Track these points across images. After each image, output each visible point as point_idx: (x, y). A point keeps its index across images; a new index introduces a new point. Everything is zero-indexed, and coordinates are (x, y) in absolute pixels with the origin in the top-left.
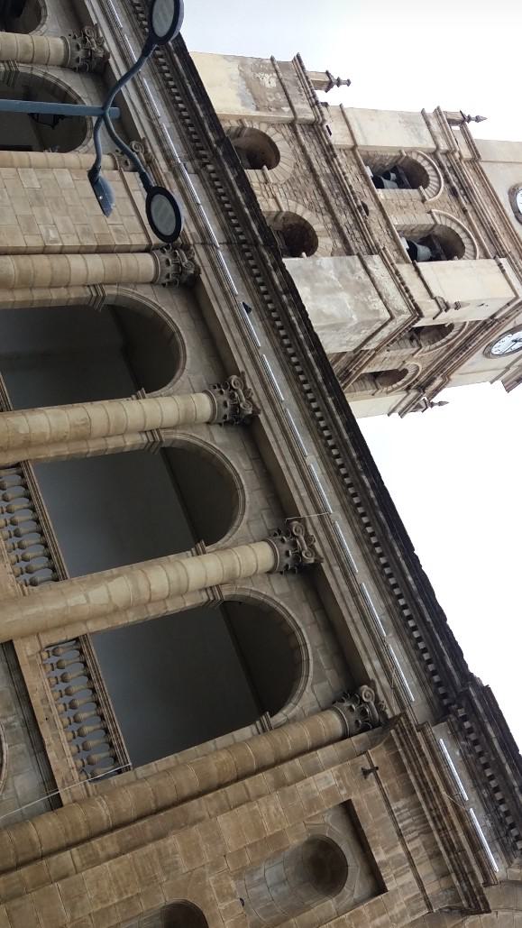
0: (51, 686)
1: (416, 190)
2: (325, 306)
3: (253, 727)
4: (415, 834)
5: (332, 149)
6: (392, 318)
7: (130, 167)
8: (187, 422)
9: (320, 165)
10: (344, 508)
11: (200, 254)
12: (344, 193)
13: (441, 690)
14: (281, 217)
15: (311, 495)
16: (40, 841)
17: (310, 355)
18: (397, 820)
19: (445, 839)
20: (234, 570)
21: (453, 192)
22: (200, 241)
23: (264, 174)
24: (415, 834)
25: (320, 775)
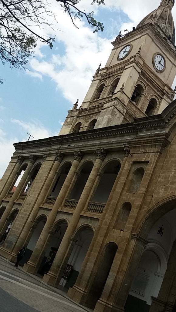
1: (104, 88)
6: (114, 106)
8: (76, 167)
10: (101, 139)
12: (92, 109)
13: (135, 131)
14: (89, 127)
17: (78, 136)
20: (95, 168)
21: (109, 77)
23: (81, 127)
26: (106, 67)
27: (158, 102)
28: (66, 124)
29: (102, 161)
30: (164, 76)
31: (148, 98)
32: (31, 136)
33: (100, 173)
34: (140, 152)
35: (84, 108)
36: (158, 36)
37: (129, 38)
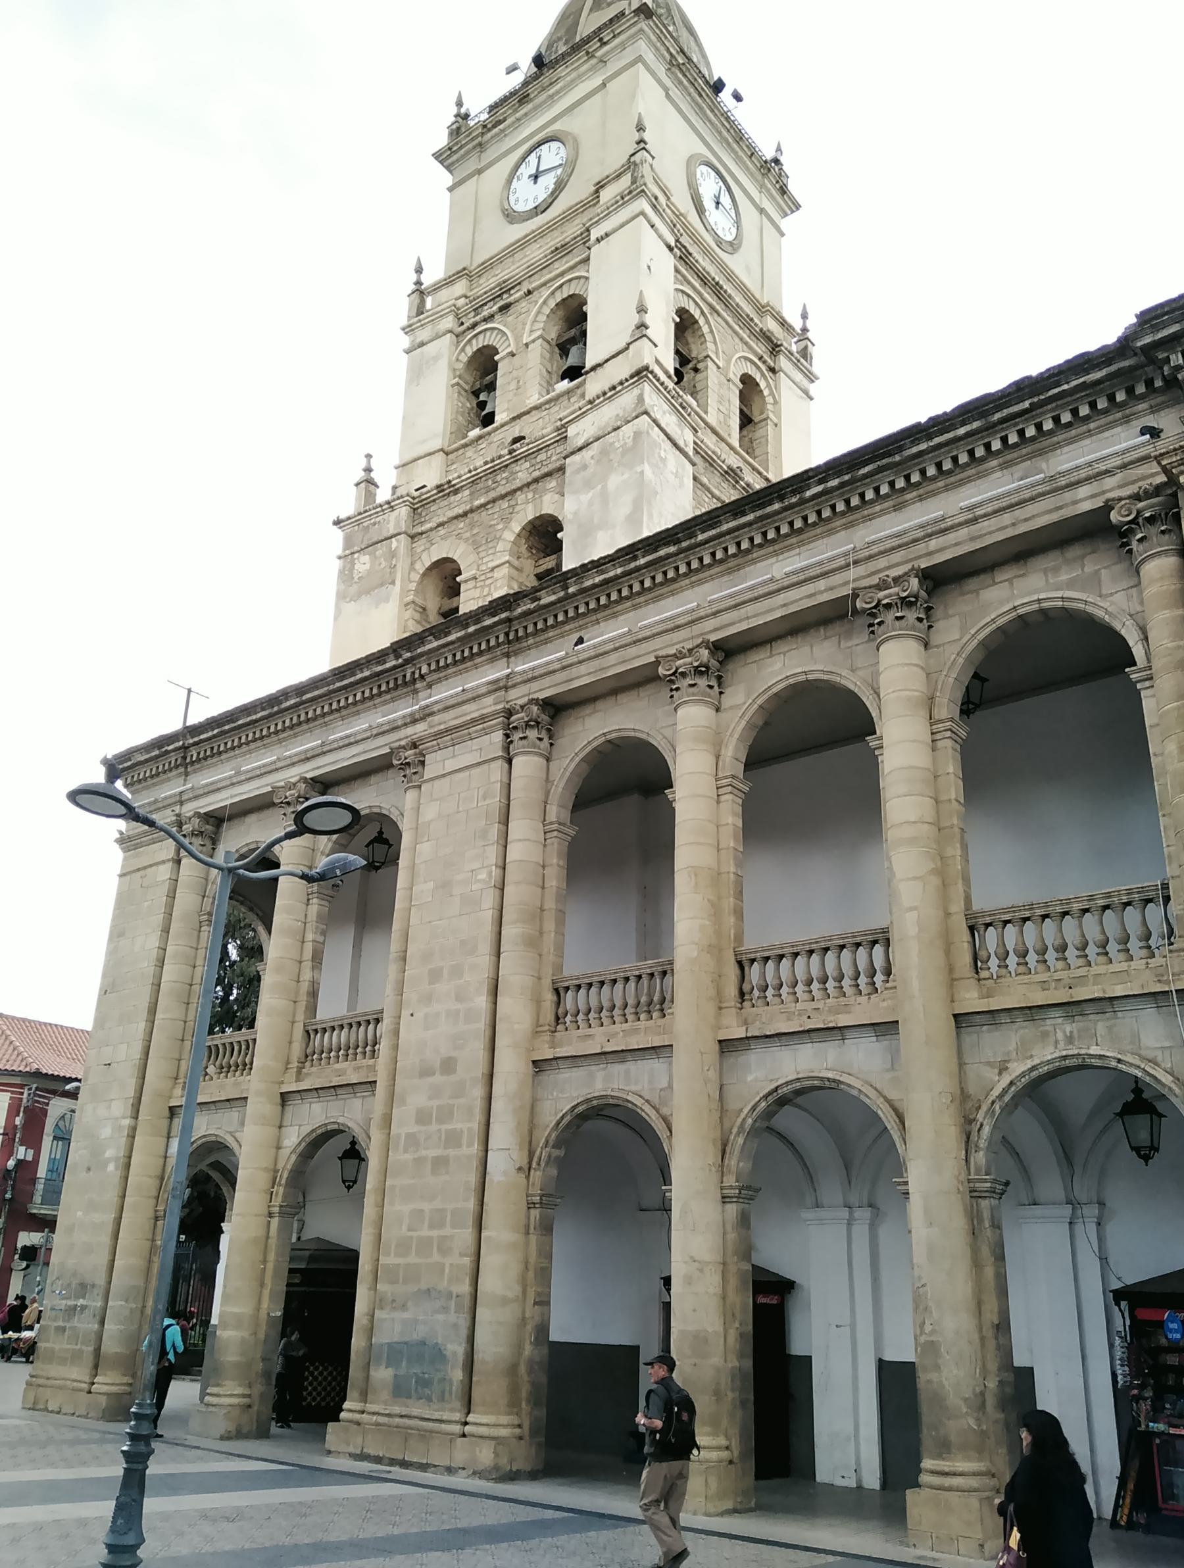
1: (500, 365)
3: (1143, 694)
5: (442, 485)
6: (646, 413)
7: (420, 769)
9: (459, 503)
11: (518, 696)
13: (1140, 389)
14: (516, 563)
15: (824, 575)
17: (642, 561)
21: (505, 308)
22: (502, 693)
23: (466, 581)
26: (460, 268)
27: (766, 393)
28: (355, 587)
29: (922, 649)
31: (732, 376)
32: (190, 691)
33: (952, 719)
36: (680, 76)
37: (530, 106)
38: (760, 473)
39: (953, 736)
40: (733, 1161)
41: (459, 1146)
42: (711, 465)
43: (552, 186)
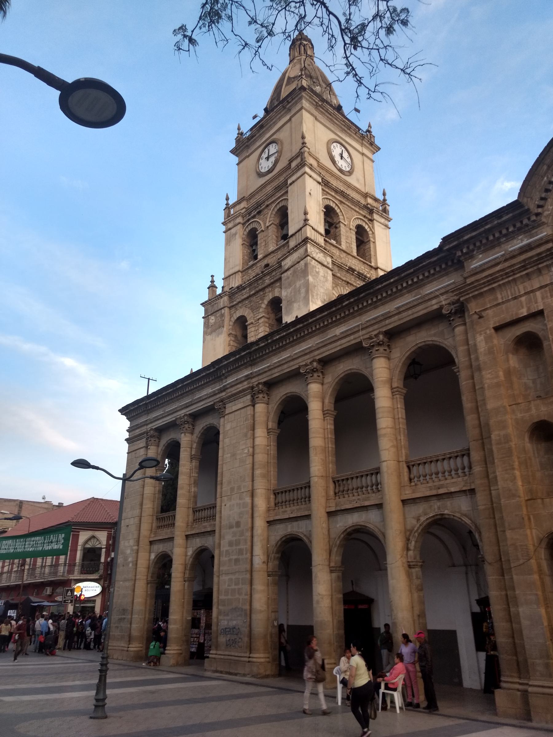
0: (428, 483)
1: (259, 236)
2: (302, 295)
3: (459, 376)
4: (516, 288)
6: (308, 255)
9: (245, 294)
10: (360, 315)
11: (255, 381)
12: (257, 280)
13: (450, 263)
16: (485, 505)
17: (292, 330)
18: (507, 299)
19: (519, 271)
21: (259, 213)
23: (250, 324)
24: (516, 288)
25: (478, 344)
27: (368, 230)
29: (387, 361)
30: (358, 180)
31: (351, 227)
32: (149, 379)
34: (500, 301)
35: (236, 285)
36: (321, 109)
37: (264, 129)
38: (367, 264)
39: (399, 393)
40: (333, 557)
41: (242, 554)
42: (341, 268)
43: (273, 162)
